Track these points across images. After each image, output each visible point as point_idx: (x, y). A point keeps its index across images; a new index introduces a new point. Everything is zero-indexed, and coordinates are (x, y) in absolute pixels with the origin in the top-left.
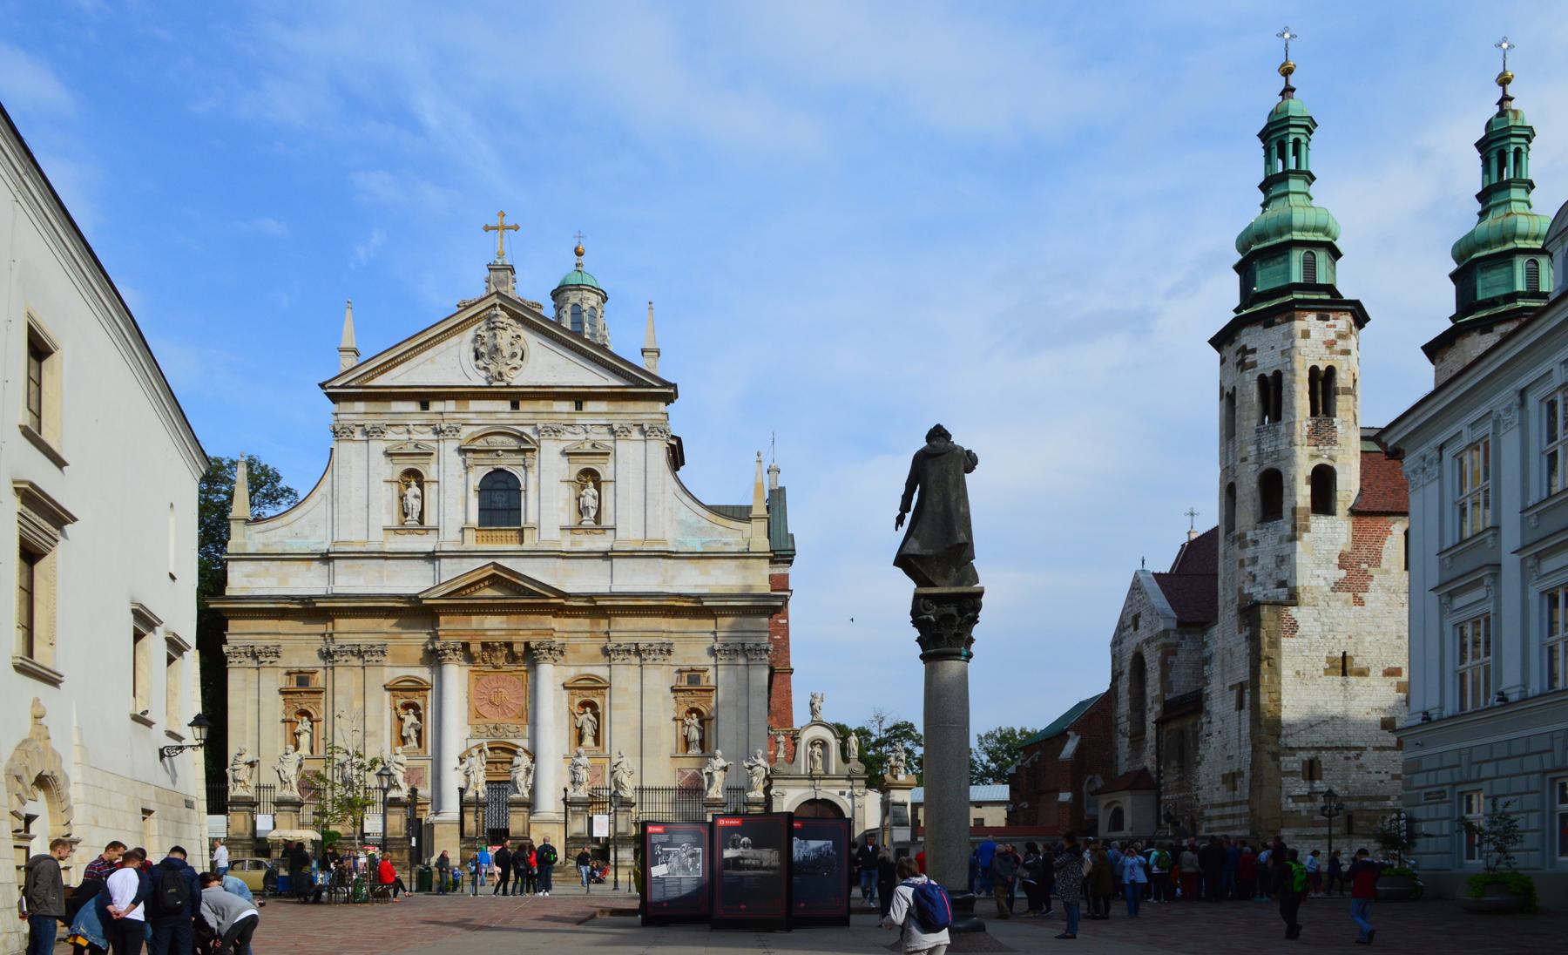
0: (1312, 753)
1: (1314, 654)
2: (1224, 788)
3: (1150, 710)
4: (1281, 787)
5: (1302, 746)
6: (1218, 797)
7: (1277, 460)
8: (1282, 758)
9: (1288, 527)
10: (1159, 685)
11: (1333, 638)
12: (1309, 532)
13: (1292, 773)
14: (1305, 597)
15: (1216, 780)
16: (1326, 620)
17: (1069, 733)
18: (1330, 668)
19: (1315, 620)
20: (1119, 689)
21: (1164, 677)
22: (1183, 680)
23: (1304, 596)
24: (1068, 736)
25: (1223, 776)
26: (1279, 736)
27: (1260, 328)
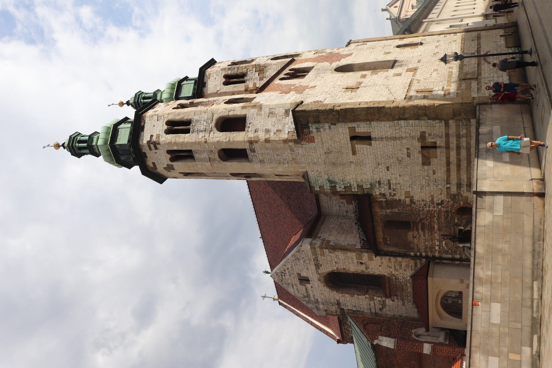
2: (434, 161)
3: (367, 268)
9: (253, 111)
10: (349, 254)
12: (260, 102)
15: (426, 173)
16: (318, 94)
17: (375, 343)
20: (350, 308)
21: (344, 249)
23: (299, 101)
24: (377, 344)
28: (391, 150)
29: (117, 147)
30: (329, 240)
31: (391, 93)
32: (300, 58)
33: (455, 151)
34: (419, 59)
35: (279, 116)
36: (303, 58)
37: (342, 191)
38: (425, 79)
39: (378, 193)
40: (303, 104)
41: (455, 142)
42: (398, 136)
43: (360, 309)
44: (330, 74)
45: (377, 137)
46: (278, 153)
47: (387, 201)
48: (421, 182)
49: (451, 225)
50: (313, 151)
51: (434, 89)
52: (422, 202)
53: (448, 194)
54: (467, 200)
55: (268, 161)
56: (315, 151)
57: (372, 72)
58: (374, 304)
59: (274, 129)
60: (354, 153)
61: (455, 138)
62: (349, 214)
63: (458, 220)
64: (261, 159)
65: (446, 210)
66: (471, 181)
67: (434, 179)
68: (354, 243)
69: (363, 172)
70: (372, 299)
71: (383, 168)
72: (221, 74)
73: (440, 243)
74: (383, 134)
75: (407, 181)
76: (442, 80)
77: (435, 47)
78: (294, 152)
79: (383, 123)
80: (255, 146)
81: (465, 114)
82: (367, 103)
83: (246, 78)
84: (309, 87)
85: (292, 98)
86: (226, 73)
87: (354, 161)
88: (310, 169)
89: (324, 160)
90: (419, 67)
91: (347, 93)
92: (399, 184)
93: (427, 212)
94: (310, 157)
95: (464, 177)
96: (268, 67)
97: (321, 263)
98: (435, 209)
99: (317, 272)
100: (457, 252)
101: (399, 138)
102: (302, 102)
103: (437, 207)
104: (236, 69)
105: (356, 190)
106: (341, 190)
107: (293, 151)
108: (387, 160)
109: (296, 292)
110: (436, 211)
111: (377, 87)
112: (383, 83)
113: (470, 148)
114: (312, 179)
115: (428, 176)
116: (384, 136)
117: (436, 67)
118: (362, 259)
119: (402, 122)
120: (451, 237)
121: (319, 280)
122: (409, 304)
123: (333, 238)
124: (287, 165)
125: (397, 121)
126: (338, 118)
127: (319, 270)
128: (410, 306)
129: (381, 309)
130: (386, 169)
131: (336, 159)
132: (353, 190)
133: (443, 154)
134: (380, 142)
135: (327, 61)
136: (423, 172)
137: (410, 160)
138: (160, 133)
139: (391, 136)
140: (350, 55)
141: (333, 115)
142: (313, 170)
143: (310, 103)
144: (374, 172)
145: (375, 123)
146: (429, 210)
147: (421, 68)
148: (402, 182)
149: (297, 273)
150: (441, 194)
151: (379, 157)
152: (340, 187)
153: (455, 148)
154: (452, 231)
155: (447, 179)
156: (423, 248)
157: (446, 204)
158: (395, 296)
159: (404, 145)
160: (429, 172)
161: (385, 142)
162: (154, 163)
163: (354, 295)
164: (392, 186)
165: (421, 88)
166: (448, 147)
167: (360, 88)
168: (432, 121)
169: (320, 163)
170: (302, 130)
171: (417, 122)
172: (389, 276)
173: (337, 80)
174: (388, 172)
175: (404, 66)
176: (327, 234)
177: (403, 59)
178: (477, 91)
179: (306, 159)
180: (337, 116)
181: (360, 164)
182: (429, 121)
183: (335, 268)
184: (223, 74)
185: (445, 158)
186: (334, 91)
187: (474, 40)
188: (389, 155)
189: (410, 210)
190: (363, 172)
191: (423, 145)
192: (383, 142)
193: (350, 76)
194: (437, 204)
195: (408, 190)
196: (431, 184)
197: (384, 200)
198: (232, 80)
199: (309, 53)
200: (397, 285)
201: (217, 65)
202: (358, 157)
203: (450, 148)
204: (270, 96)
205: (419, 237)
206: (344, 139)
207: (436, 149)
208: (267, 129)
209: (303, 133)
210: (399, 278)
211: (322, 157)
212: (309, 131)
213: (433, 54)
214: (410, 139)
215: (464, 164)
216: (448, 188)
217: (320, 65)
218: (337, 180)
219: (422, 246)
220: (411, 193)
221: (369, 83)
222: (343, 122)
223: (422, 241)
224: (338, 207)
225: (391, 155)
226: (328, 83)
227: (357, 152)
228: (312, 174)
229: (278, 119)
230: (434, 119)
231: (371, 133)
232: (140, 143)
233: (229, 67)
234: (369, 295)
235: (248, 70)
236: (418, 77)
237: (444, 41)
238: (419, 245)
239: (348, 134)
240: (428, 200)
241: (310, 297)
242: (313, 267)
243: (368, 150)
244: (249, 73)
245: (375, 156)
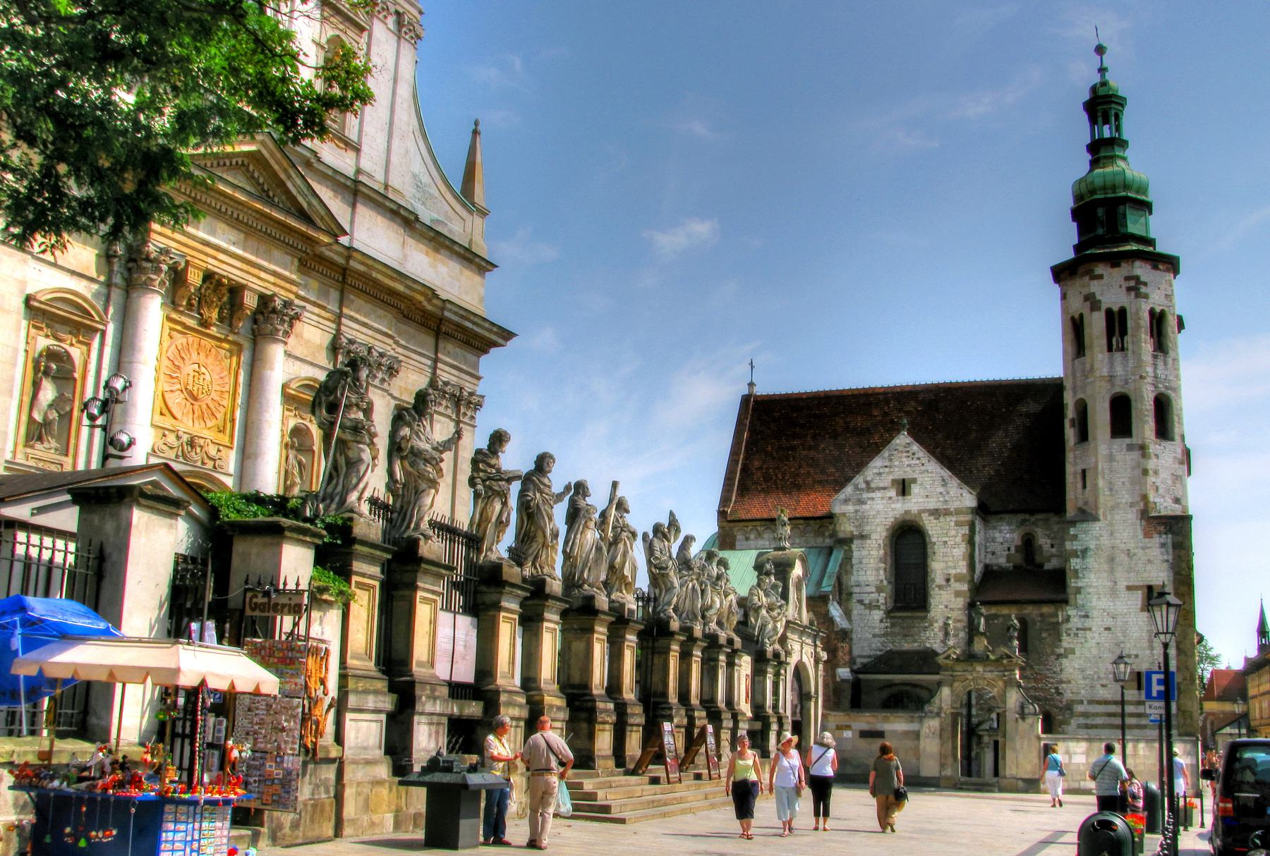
3: (940, 587)
6: (1103, 694)
7: (1167, 388)
15: (1102, 675)
20: (856, 554)
29: (1121, 208)
47: (1058, 623)
53: (1072, 701)
59: (1158, 482)
60: (1129, 588)
62: (989, 556)
70: (879, 590)
95: (1099, 721)
97: (942, 519)
99: (921, 512)
105: (1073, 585)
109: (875, 471)
118: (956, 581)
121: (907, 512)
123: (977, 539)
129: (861, 602)
138: (1150, 300)
148: (1086, 645)
150: (1073, 693)
162: (1101, 277)
181: (1113, 592)
183: (934, 540)
196: (1087, 682)
197: (1060, 620)
211: (1123, 545)
216: (1082, 702)
224: (1001, 540)
232: (1138, 264)
239: (1157, 583)
240: (1064, 676)
242: (932, 505)
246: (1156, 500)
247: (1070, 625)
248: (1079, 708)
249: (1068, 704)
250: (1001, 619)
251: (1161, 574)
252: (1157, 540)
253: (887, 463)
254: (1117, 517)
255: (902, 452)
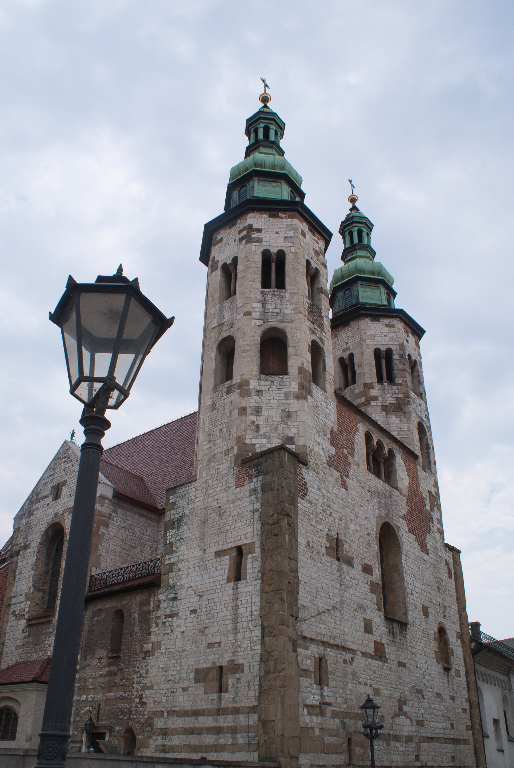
0: (321, 648)
1: (319, 526)
2: (201, 688)
4: (299, 691)
5: (313, 637)
8: (299, 650)
11: (330, 515)
13: (305, 672)
14: (311, 460)
15: (184, 676)
16: (325, 492)
18: (329, 548)
19: (318, 488)
22: (111, 556)
23: (312, 461)
25: (197, 671)
26: (297, 618)
27: (265, 216)
28: (220, 615)
30: (110, 526)
31: (319, 614)
32: (419, 468)
33: (213, 725)
34: (407, 665)
35: (283, 427)
36: (419, 474)
37: (167, 540)
38: (354, 674)
39: (160, 599)
40: (301, 465)
41: (226, 725)
42: (239, 626)
43: (16, 580)
44: (377, 515)
45: (239, 590)
46: (225, 431)
48: (172, 669)
49: (112, 719)
50: (223, 487)
51: (326, 688)
52: (144, 671)
53: (154, 713)
54: (144, 747)
55: (214, 416)
56: (223, 491)
57: (378, 584)
58: (21, 601)
59: (260, 420)
60: (218, 554)
61: (232, 724)
63: (118, 731)
64: (217, 405)
65: (132, 711)
66: (170, 752)
67: (176, 688)
68: (103, 565)
69: (191, 571)
71: (194, 604)
72: (393, 344)
73: (90, 701)
74: (242, 601)
75: (175, 645)
76: (350, 703)
77: (437, 693)
78: (223, 455)
79: (258, 599)
80: (235, 395)
81: (265, 741)
82: (296, 571)
83: (386, 384)
84: (345, 478)
85: (317, 449)
86: (394, 353)
87: (207, 555)
88: (200, 485)
89: (210, 506)
90: (386, 664)
91: (325, 539)
92: (172, 631)
93: (132, 679)
94: (215, 482)
95: (176, 741)
96: (405, 417)
98: (135, 693)
99: (64, 511)
100: (76, 730)
101: (235, 628)
102: (306, 464)
103: (138, 696)
104: (401, 367)
105: (167, 562)
106: (168, 538)
107: (225, 455)
108: (204, 610)
110: (133, 694)
111: (336, 591)
112: (348, 601)
113: (216, 752)
114: (185, 489)
115: (180, 679)
116: (240, 603)
117: (385, 692)
119: (257, 633)
120: (95, 721)
121: (56, 514)
122: (18, 656)
124: (206, 447)
125: (260, 624)
126: (268, 524)
127: (68, 513)
128: (14, 657)
129: (14, 612)
130: (192, 609)
131: (211, 525)
132: (167, 557)
133: (210, 703)
134: (232, 597)
135: (409, 512)
136: (185, 671)
137: (203, 648)
139: (240, 615)
140: (424, 549)
141: (273, 513)
142: (198, 489)
143: (304, 476)
144: (190, 589)
145: (259, 585)
146: (134, 683)
147: (385, 668)
148: (173, 636)
149: (66, 480)
150: (155, 702)
151: (211, 597)
152: (172, 535)
153: (218, 725)
154: (104, 722)
155: (174, 711)
156: (85, 675)
157: (141, 711)
158: (28, 634)
159: (226, 637)
160: (185, 681)
161: (231, 604)
163: (34, 570)
164: (170, 619)
165: (329, 665)
166: (220, 712)
167: (337, 563)
168: (258, 683)
169: (207, 500)
170: (254, 465)
171: (258, 658)
172: (53, 622)
173: (360, 526)
174: (189, 612)
175: (390, 638)
176: (122, 523)
177: (408, 637)
178: (317, 764)
179: (213, 476)
180: (271, 522)
182: (258, 679)
184: (393, 348)
185: (204, 707)
186: (332, 518)
187: (453, 761)
188: (212, 612)
189: (136, 651)
190: (191, 571)
191: (224, 670)
192: (231, 601)
193: (370, 546)
194: (142, 695)
195: (163, 647)
197: (151, 609)
198: (383, 362)
199: (433, 483)
200: (42, 635)
201: (412, 339)
202: (212, 561)
203: (218, 717)
204: (326, 415)
205: (100, 667)
206: (238, 536)
207: (217, 692)
208: (262, 409)
209: (250, 467)
210: (51, 638)
211: (215, 503)
212: (252, 477)
213: (419, 688)
214: (234, 647)
215: (194, 740)
217: (403, 502)
218: (182, 529)
219: (88, 672)
220: (158, 651)
221: (348, 578)
222: (262, 532)
223: (94, 673)
225: (212, 616)
226: (353, 510)
227: (218, 559)
228: (192, 488)
229: (279, 426)
230: (261, 686)
231: (244, 581)
233: (407, 357)
234: (33, 592)
235: (399, 387)
236: (360, 662)
237: (454, 708)
238: (90, 667)
239: (245, 542)
241: (36, 503)
243: (220, 578)
244: (394, 387)
245: (212, 590)
246: (254, 441)
247: (161, 613)
248: (159, 723)
249: (149, 718)
250: (103, 614)
251: (250, 530)
252: (249, 486)
253: (51, 473)
254: (213, 471)
255: (62, 459)
